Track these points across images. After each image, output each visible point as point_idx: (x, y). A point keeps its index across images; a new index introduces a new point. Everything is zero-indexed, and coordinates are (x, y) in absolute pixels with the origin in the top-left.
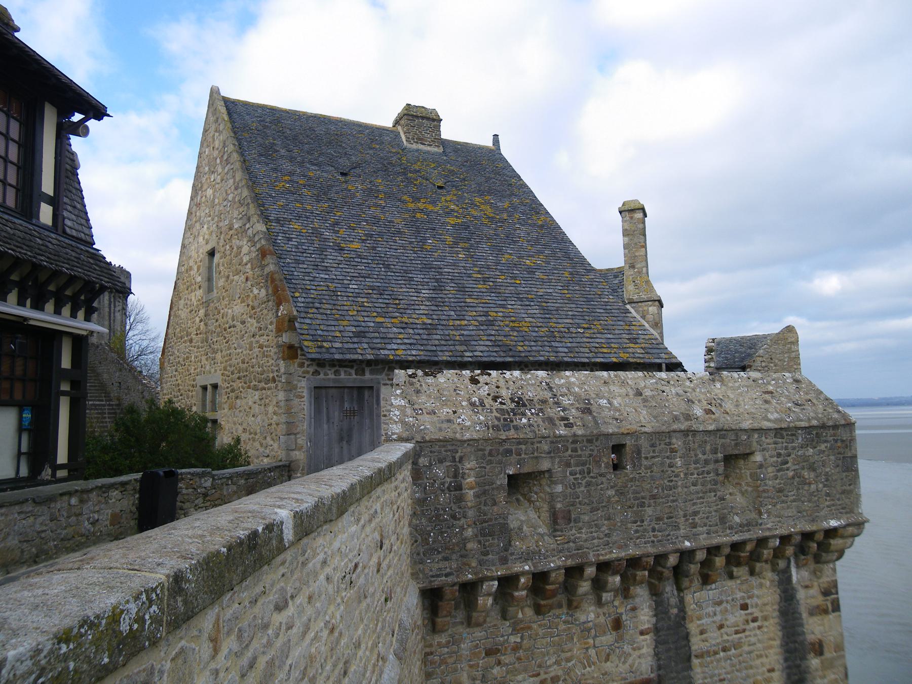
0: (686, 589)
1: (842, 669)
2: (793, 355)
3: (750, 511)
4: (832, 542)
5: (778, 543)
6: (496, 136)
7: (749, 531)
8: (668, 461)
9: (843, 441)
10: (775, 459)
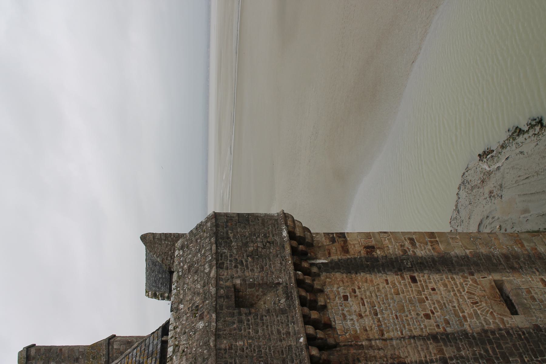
0: (335, 341)
1: (382, 235)
2: (163, 237)
3: (277, 290)
5: (300, 273)
7: (291, 292)
8: (239, 352)
9: (227, 222)
10: (239, 270)
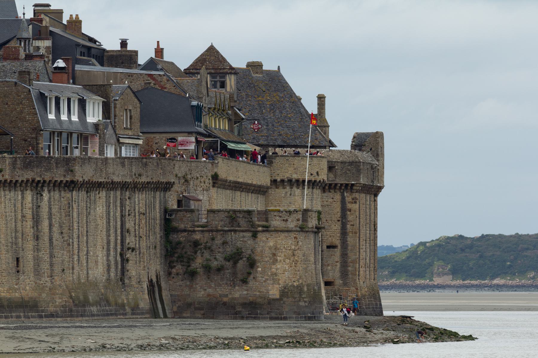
1: (355, 216)
4: (354, 187)
6: (279, 67)
